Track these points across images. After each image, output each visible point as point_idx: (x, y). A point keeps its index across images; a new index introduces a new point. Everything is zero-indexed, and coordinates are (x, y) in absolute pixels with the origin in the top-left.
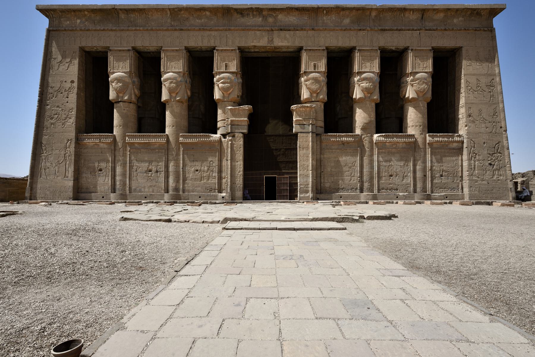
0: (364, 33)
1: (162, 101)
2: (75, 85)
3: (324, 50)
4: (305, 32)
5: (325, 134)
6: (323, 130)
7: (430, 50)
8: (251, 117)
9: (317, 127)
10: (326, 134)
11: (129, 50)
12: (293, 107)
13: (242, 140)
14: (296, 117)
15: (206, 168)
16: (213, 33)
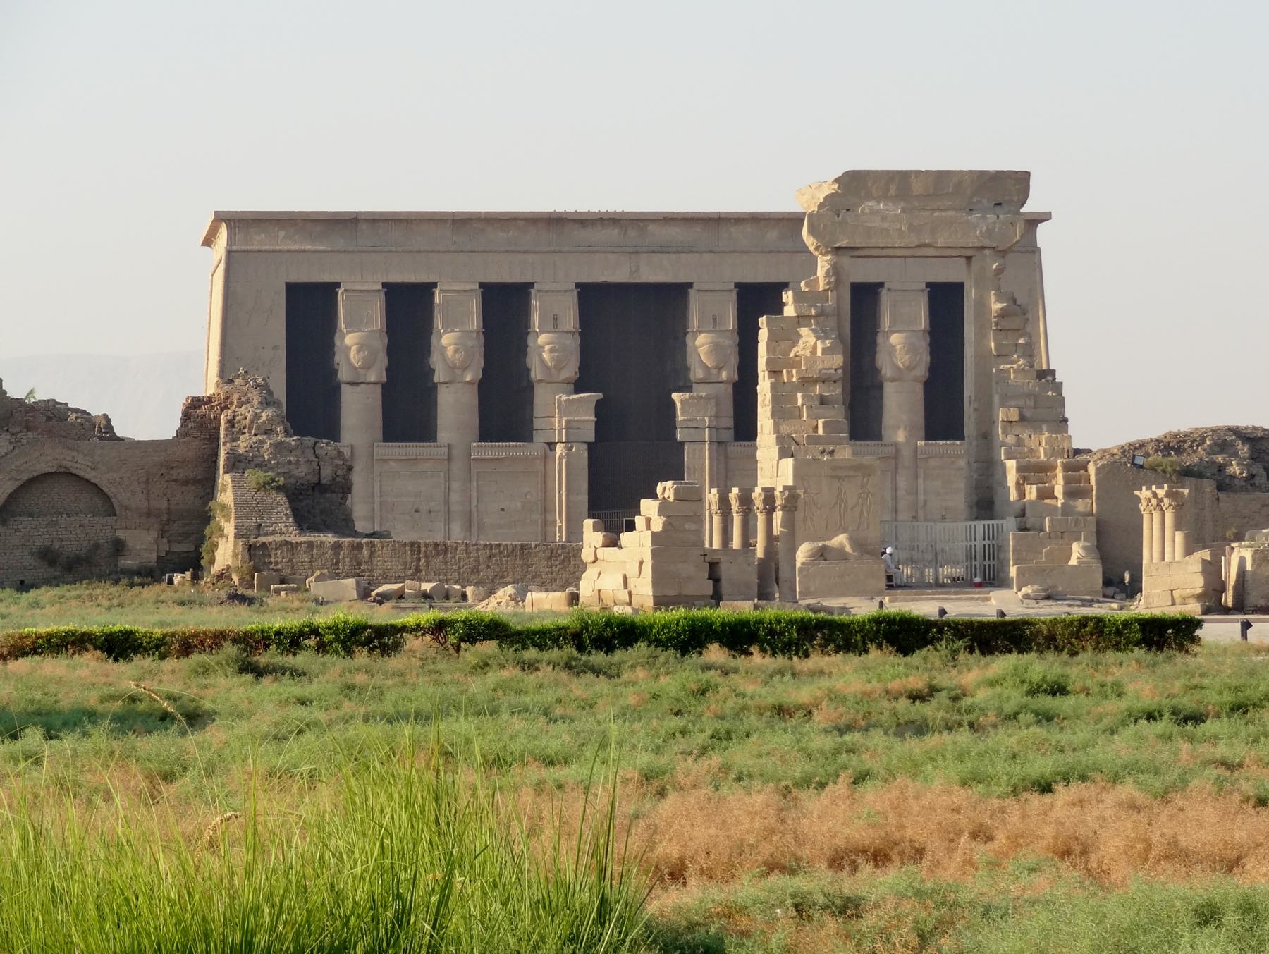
0: (804, 258)
1: (436, 380)
2: (282, 353)
3: (730, 291)
4: (697, 255)
5: (733, 444)
6: (732, 432)
7: (922, 290)
8: (600, 407)
9: (720, 431)
10: (736, 443)
11: (378, 291)
12: (675, 396)
13: (586, 455)
14: (682, 415)
15: (519, 505)
16: (530, 257)
